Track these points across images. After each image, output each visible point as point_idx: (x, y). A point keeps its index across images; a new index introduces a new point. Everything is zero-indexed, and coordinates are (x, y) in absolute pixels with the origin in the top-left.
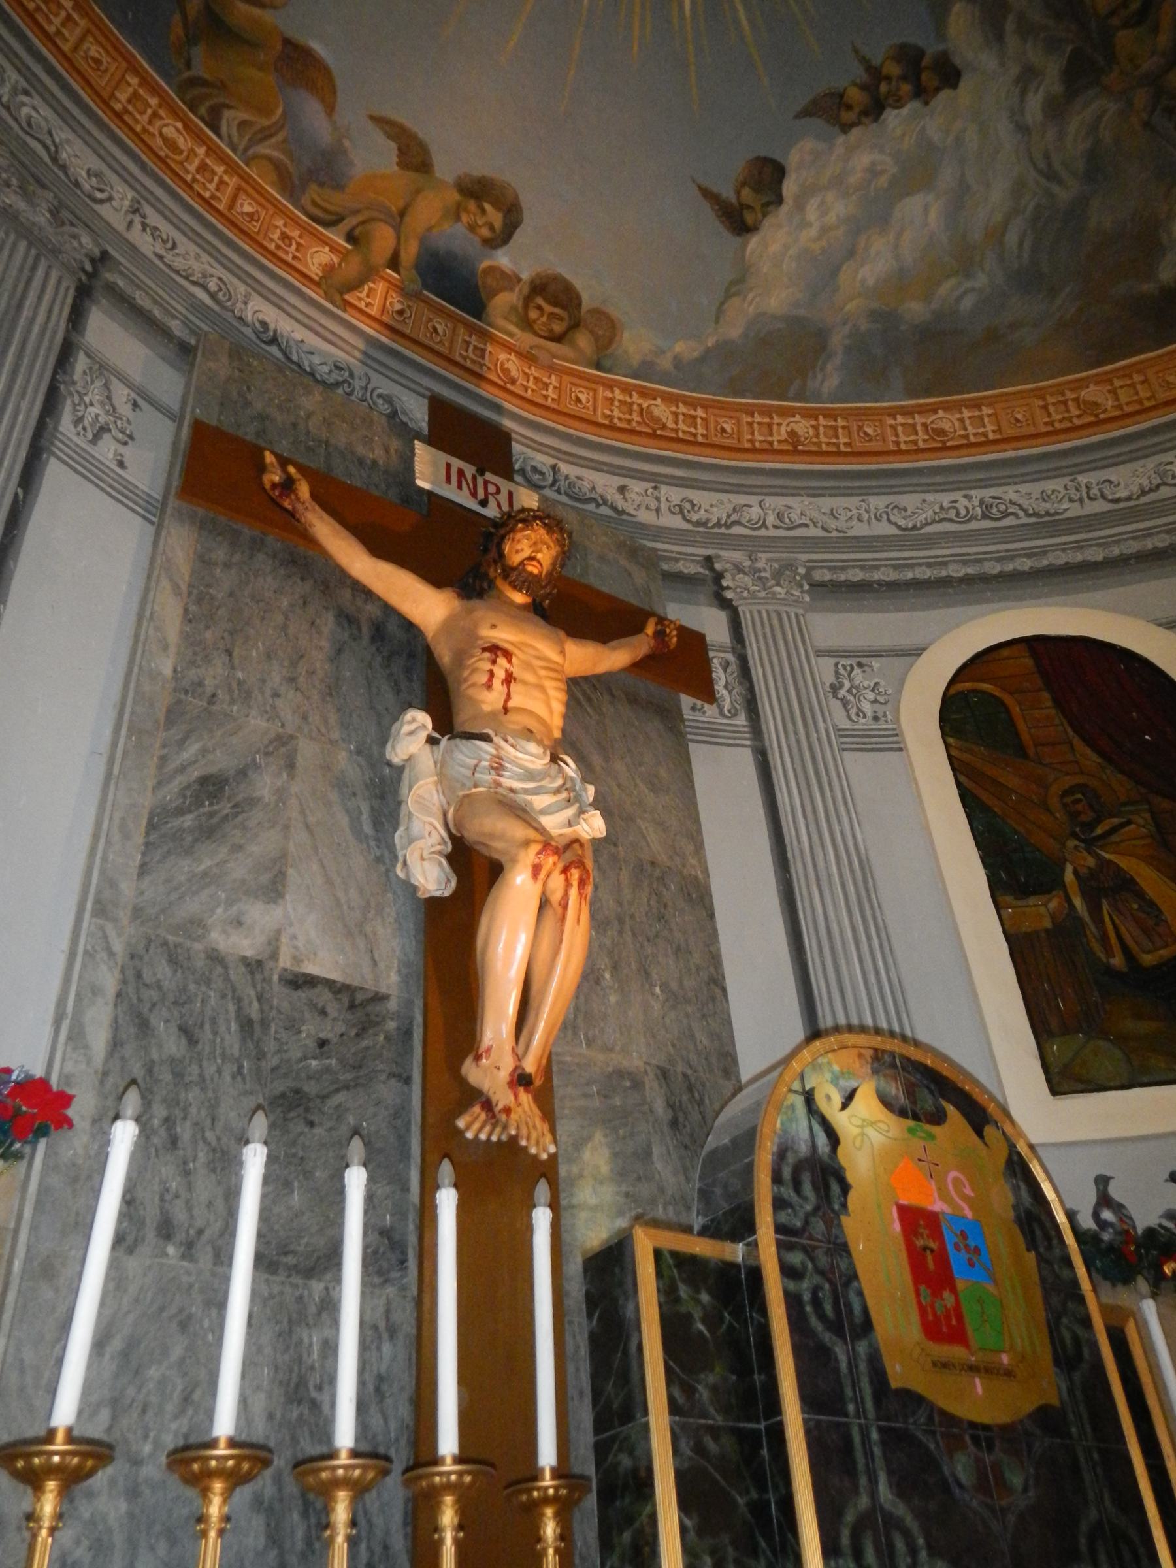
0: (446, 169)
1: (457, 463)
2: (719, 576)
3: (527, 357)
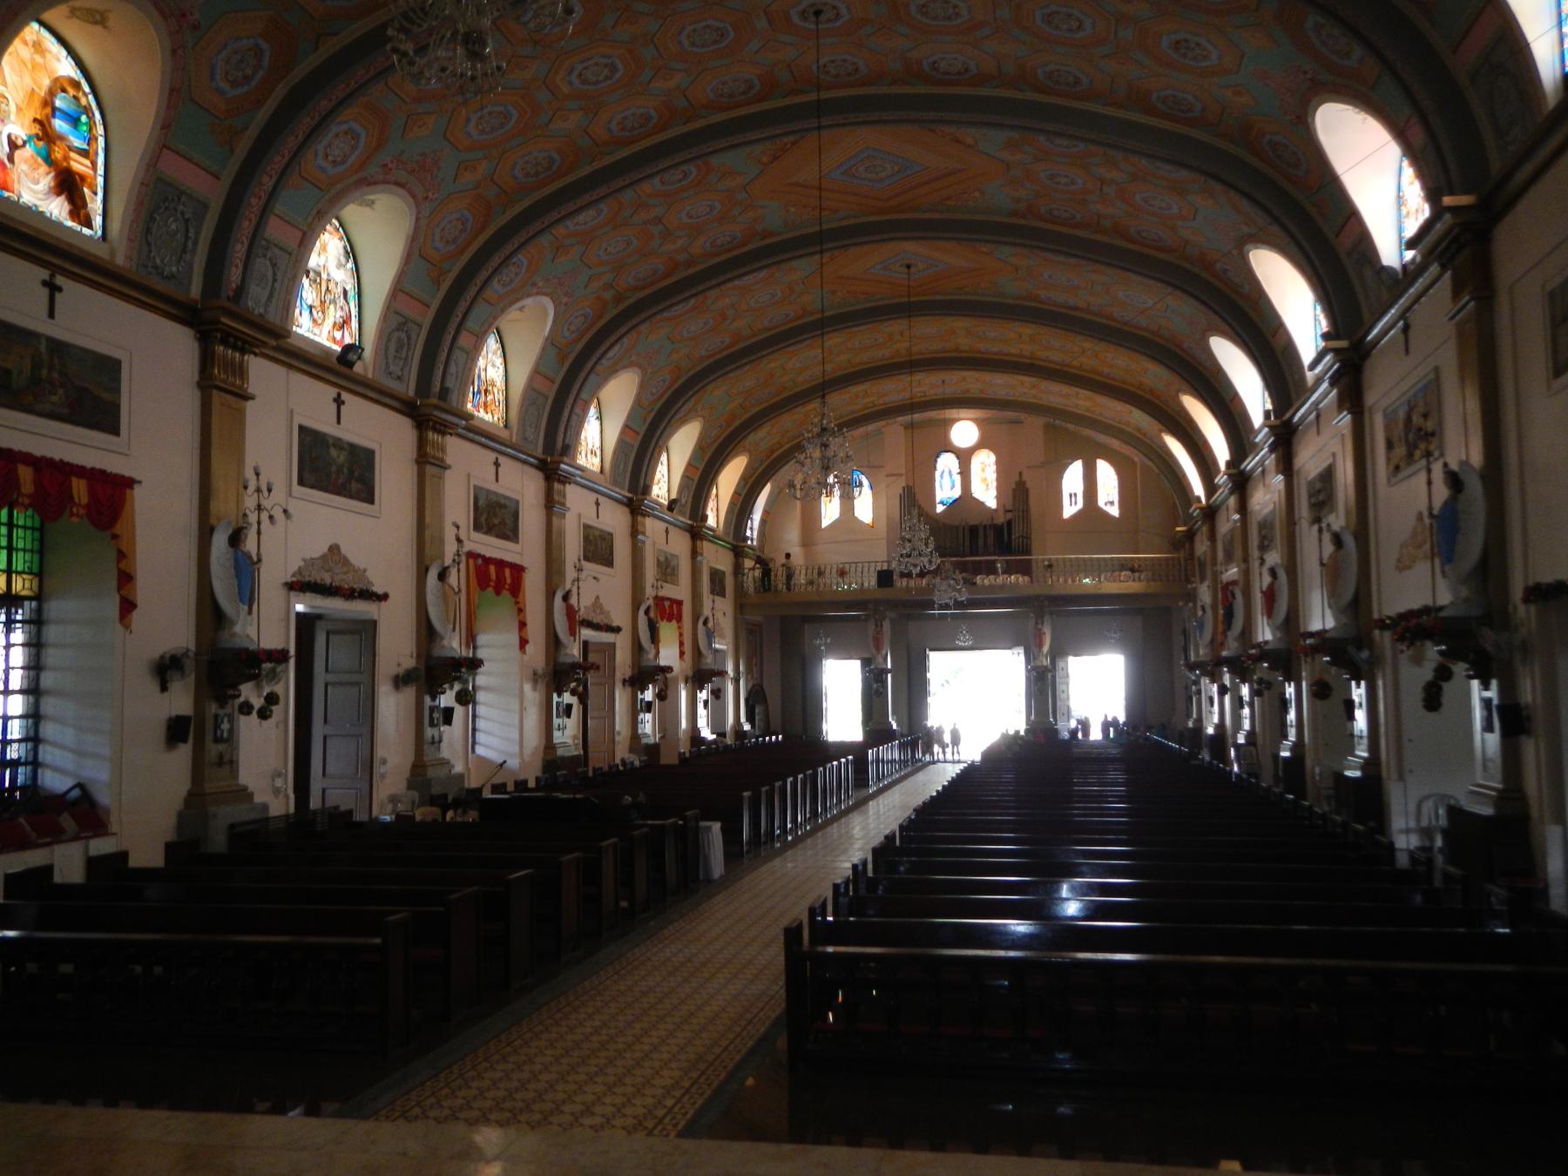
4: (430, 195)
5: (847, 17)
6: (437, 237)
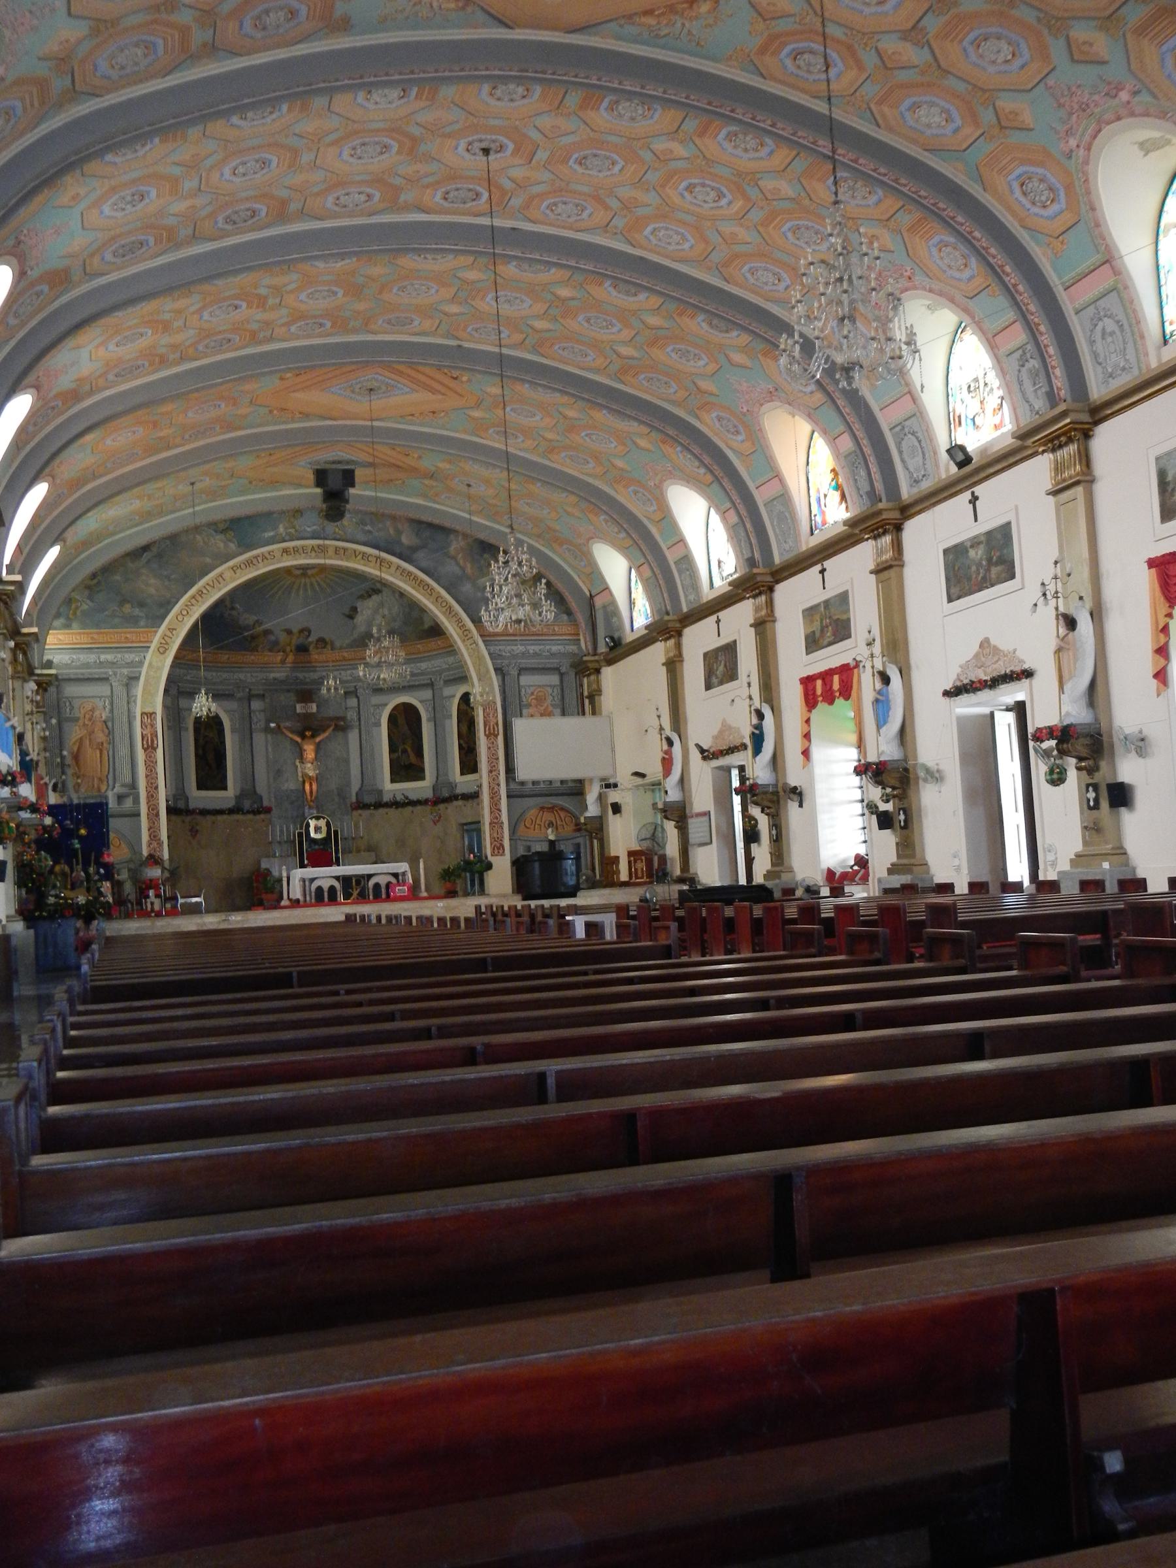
0: (295, 631)
1: (303, 705)
3: (319, 654)
4: (908, 274)
5: (462, 141)
6: (957, 275)
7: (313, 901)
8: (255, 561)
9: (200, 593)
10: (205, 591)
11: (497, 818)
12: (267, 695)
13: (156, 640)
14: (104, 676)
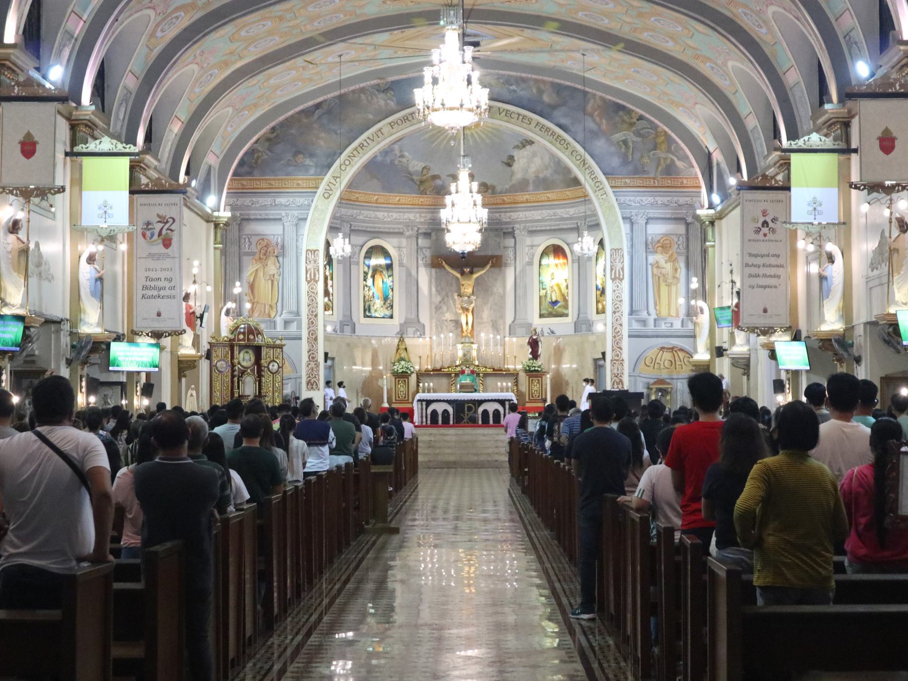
2: (514, 231)
7: (429, 422)
8: (410, 118)
9: (361, 146)
10: (365, 144)
11: (618, 355)
12: (433, 234)
13: (323, 186)
14: (278, 217)
